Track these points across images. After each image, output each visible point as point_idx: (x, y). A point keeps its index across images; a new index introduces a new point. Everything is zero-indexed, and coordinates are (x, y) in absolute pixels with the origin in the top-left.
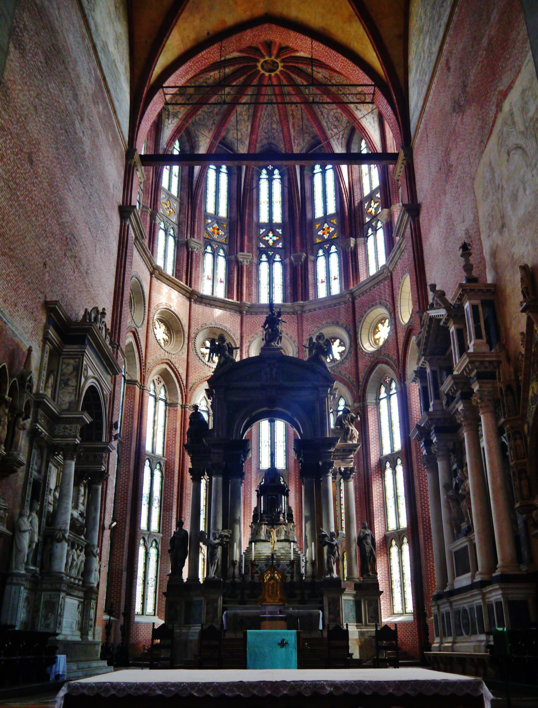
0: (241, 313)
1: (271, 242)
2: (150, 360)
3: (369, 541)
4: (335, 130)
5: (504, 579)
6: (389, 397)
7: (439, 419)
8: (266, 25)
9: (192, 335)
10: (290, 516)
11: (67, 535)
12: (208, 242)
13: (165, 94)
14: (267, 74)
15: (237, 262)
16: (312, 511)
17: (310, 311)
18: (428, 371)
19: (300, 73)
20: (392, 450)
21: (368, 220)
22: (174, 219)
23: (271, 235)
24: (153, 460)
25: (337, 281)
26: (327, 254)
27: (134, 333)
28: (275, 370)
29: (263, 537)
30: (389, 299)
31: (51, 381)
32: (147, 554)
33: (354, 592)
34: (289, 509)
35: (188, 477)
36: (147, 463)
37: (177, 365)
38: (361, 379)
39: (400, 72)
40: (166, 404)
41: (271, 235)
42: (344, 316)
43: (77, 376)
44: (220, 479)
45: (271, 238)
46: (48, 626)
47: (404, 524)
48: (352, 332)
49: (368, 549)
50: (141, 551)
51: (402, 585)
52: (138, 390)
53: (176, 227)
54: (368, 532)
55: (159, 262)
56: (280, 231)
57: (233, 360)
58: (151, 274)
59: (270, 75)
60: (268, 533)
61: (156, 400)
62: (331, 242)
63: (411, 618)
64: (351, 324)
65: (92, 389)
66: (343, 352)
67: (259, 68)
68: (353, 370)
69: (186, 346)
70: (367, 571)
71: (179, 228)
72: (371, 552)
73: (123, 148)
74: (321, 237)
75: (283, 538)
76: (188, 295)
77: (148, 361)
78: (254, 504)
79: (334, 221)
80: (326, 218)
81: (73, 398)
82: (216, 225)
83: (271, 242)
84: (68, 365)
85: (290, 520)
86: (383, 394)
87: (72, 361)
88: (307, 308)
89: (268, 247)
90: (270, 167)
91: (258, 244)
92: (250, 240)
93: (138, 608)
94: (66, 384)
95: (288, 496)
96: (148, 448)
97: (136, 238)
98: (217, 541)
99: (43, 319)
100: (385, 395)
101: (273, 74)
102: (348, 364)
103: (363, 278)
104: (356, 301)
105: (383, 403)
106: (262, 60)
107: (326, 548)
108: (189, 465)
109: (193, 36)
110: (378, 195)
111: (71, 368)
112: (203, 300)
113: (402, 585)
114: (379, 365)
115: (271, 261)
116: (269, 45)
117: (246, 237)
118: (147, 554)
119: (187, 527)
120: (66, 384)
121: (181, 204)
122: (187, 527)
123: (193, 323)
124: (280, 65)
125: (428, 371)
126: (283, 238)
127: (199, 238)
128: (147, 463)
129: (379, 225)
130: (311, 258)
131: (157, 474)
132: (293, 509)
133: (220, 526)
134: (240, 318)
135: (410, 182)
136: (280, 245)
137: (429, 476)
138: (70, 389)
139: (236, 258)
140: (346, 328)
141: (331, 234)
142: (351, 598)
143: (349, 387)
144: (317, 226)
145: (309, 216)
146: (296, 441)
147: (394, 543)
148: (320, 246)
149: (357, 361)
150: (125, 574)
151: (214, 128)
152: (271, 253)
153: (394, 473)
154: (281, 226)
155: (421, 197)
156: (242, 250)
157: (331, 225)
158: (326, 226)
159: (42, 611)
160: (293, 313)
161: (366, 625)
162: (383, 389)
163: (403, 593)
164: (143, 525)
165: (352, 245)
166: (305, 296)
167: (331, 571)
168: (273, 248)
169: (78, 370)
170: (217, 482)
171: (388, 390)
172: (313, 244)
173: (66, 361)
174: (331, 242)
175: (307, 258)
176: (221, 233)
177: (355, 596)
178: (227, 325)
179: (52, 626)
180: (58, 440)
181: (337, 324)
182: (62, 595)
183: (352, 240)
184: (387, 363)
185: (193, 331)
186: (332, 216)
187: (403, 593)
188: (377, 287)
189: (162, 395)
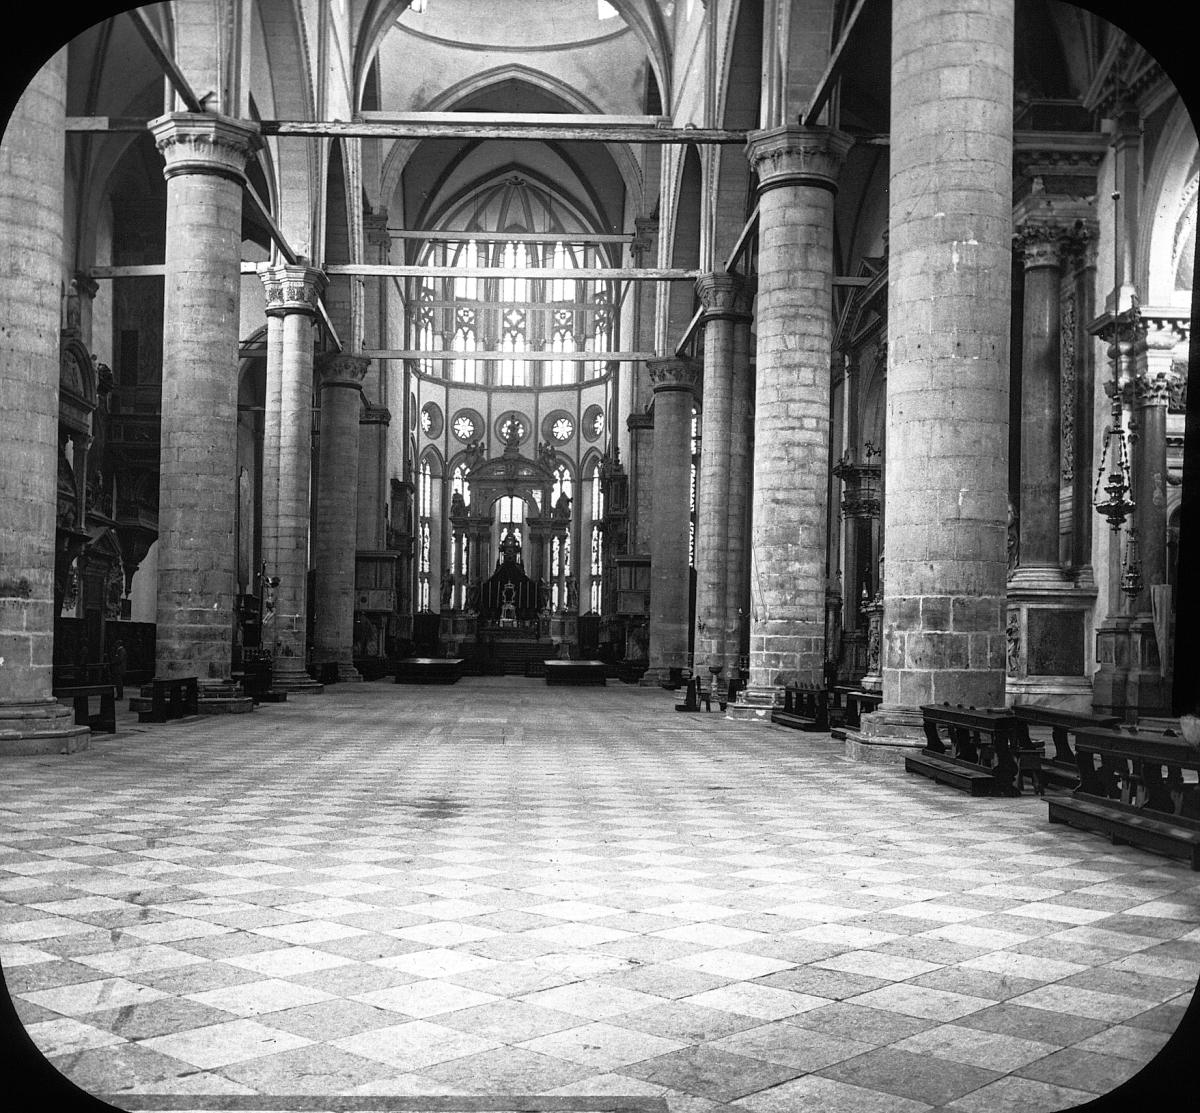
112: (457, 385)
152: (514, 333)
185: (451, 415)
189: (428, 472)
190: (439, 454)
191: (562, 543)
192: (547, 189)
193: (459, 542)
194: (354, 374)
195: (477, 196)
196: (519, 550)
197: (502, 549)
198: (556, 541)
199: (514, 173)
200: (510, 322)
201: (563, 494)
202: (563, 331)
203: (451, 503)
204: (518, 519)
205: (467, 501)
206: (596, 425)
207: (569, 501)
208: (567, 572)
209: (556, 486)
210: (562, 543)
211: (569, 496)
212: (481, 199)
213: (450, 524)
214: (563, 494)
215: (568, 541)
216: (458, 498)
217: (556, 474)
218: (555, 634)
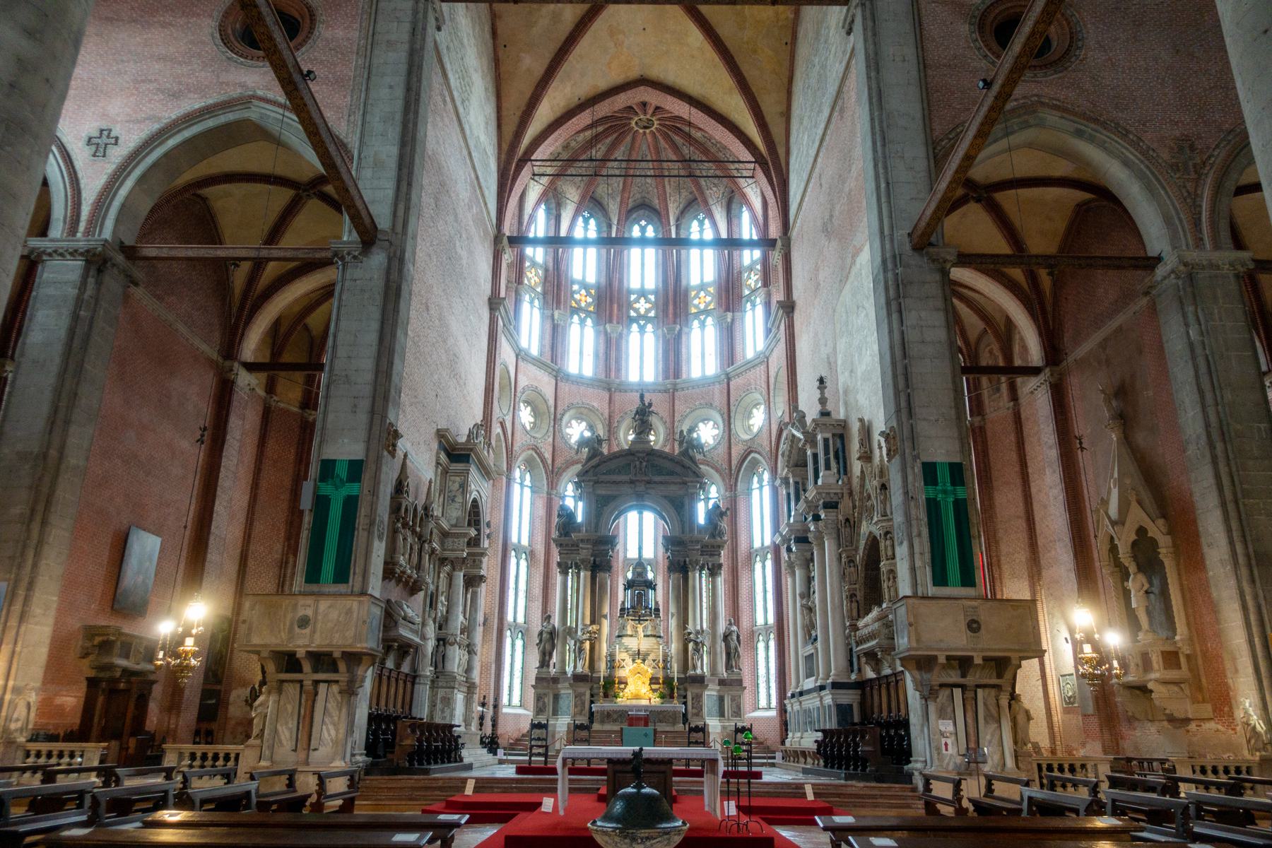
0: (609, 390)
1: (642, 311)
2: (516, 448)
3: (735, 638)
4: (715, 189)
5: (836, 686)
6: (761, 487)
7: (798, 530)
8: (642, 88)
9: (559, 416)
10: (657, 610)
11: (458, 639)
12: (576, 311)
13: (533, 166)
14: (641, 131)
15: (606, 333)
16: (678, 608)
17: (683, 389)
18: (791, 481)
19: (678, 130)
20: (763, 544)
21: (747, 292)
22: (539, 289)
23: (642, 300)
24: (518, 549)
25: (713, 357)
26: (703, 325)
27: (501, 423)
28: (644, 464)
29: (629, 632)
30: (764, 386)
31: (441, 499)
32: (513, 645)
33: (718, 688)
34: (657, 603)
35: (556, 571)
36: (513, 553)
37: (543, 450)
38: (733, 468)
39: (781, 151)
40: (533, 492)
41: (642, 300)
42: (719, 399)
43: (463, 493)
44: (589, 573)
45: (642, 306)
46: (444, 718)
47: (771, 620)
48: (726, 416)
49: (733, 645)
50: (508, 641)
51: (768, 681)
52: (504, 478)
53: (541, 297)
54: (734, 628)
55: (524, 343)
56: (652, 298)
57: (602, 453)
58: (517, 356)
59: (645, 133)
60: (635, 628)
61: (522, 485)
62: (706, 312)
63: (773, 713)
64: (726, 407)
65: (475, 501)
66: (717, 435)
67: (633, 123)
68: (726, 457)
69: (551, 429)
70: (732, 667)
71: (544, 298)
72: (736, 649)
73: (492, 232)
74: (697, 307)
75: (649, 633)
76: (554, 373)
77: (515, 448)
78: (621, 598)
79: (711, 290)
80: (702, 287)
81: (460, 513)
82: (583, 292)
83: (642, 311)
84: (454, 482)
85: (657, 616)
86: (755, 485)
87: (458, 479)
88: (679, 386)
89: (640, 317)
90: (643, 223)
91: (628, 312)
92: (620, 308)
93: (505, 700)
94: (453, 501)
95: (655, 590)
96: (514, 539)
97: (504, 325)
98: (585, 637)
99: (435, 445)
100: (758, 486)
101: (648, 131)
102: (722, 450)
103: (739, 362)
104: (732, 383)
105: (755, 494)
106: (636, 119)
107: (691, 646)
108: (556, 557)
109: (562, 104)
110: (759, 267)
111: (457, 485)
112: (568, 378)
113: (768, 681)
114: (753, 455)
115: (642, 329)
116: (644, 105)
117: (615, 306)
118: (513, 645)
119: (556, 621)
120: (453, 501)
121: (546, 270)
122: (556, 621)
123: (559, 403)
124: (656, 123)
125: (791, 481)
126: (655, 305)
127: (565, 308)
128: (513, 553)
129: (758, 300)
130: (685, 330)
131: (523, 564)
132: (661, 603)
133: (588, 622)
134: (608, 395)
135: (787, 275)
136: (652, 314)
137: (789, 580)
138: (457, 505)
139: (605, 329)
140: (720, 411)
141: (707, 304)
142: (715, 693)
143: (721, 475)
144: (693, 294)
145: (684, 283)
146: (665, 537)
147: (761, 638)
148: (697, 315)
149: (730, 448)
150: (493, 666)
151: (582, 185)
152: (642, 323)
153: (764, 567)
154: (656, 292)
155: (796, 295)
156: (611, 321)
157: (708, 293)
158: (702, 294)
159: (439, 706)
160: (665, 391)
161: (729, 719)
162: (755, 479)
163: (769, 688)
164: (510, 618)
165: (729, 320)
166: (677, 374)
167: (695, 668)
168: (645, 317)
169: (464, 487)
170: (585, 577)
171: (760, 481)
173: (452, 478)
174: (706, 312)
175: (680, 330)
176: (589, 300)
177: (719, 691)
178: (595, 404)
179: (448, 718)
180: (447, 554)
181: (711, 406)
182: (456, 691)
183: (729, 315)
184: (759, 453)
186: (709, 285)
187: (769, 688)
188: (753, 371)
189: (528, 482)
190: (543, 460)
196: (651, 585)
197: (629, 585)
200: (636, 310)
202: (702, 317)
203: (555, 520)
204: (648, 553)
205: (579, 519)
206: (751, 422)
207: (722, 514)
218: (710, 715)
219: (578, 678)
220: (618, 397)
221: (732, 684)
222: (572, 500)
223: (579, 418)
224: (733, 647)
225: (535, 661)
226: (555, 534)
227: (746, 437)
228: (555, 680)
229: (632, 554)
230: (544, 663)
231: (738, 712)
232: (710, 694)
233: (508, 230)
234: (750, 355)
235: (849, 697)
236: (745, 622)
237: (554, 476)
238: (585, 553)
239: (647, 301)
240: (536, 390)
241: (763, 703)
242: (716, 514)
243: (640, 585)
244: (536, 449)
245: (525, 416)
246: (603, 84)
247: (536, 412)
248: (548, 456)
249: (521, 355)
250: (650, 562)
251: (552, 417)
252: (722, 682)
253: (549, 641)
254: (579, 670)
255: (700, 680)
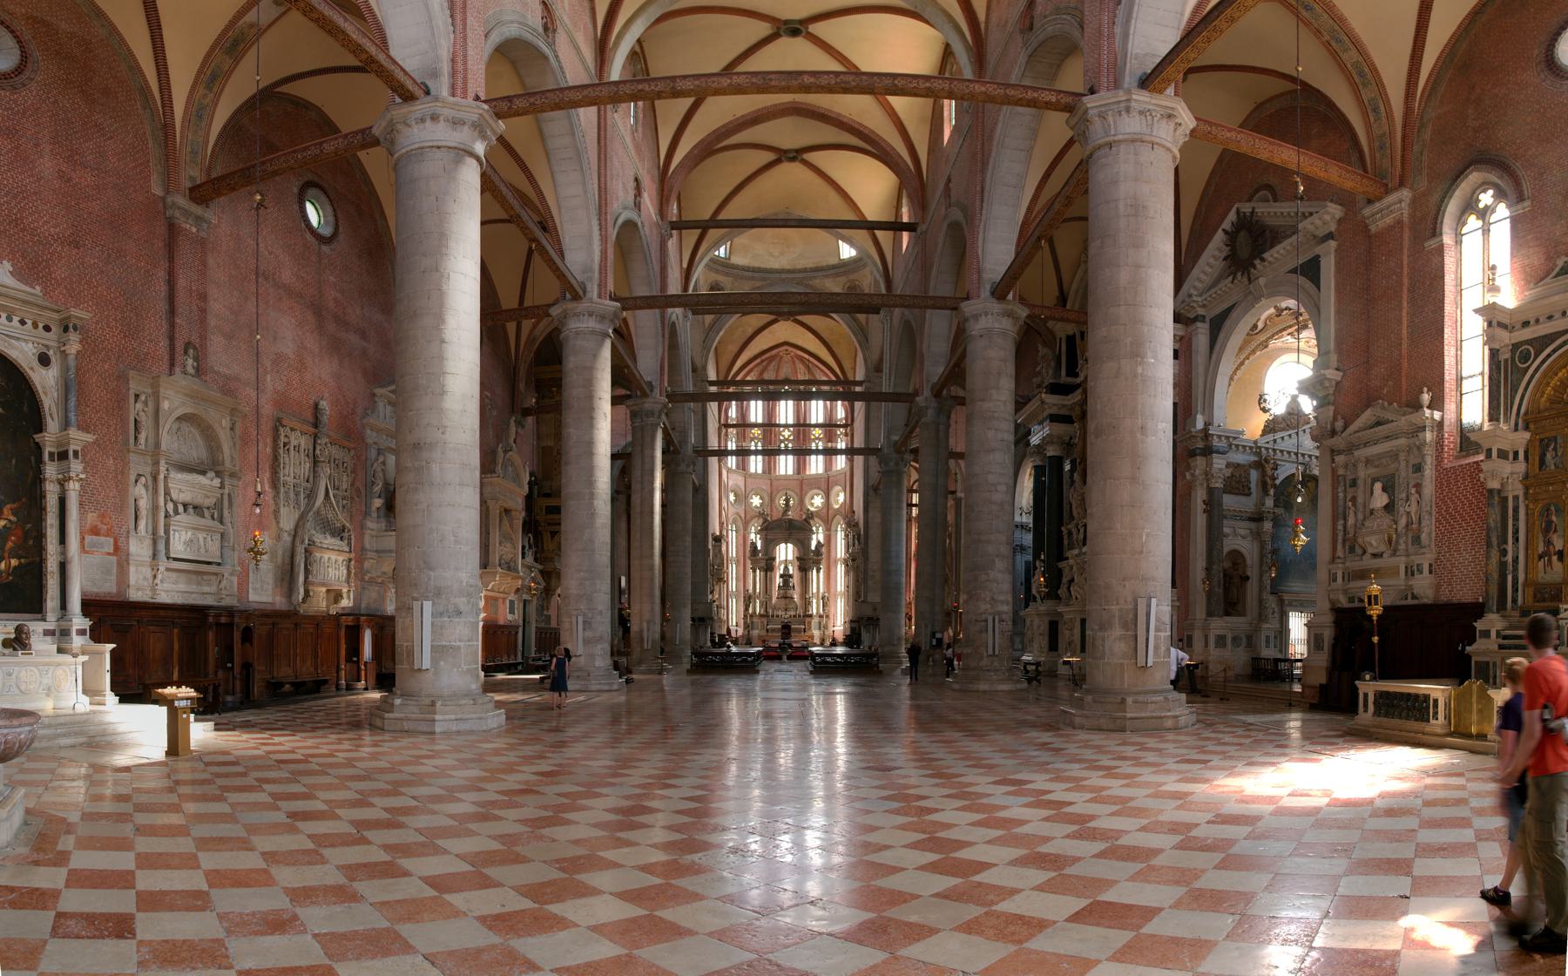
12: (752, 439)
42: (824, 486)
89: (787, 440)
92: (775, 436)
102: (825, 511)
103: (834, 469)
112: (751, 475)
119: (751, 591)
122: (751, 591)
136: (791, 438)
148: (814, 440)
172: (810, 439)
181: (819, 488)
190: (740, 517)
191: (818, 571)
192: (807, 356)
193: (754, 571)
194: (688, 466)
195: (763, 361)
196: (791, 576)
197: (781, 576)
198: (815, 571)
199: (785, 347)
201: (819, 542)
203: (748, 549)
204: (790, 557)
205: (759, 548)
208: (821, 591)
209: (814, 537)
210: (818, 571)
211: (822, 541)
212: (764, 364)
213: (749, 562)
214: (819, 542)
215: (822, 571)
216: (754, 545)
217: (814, 529)
219: (761, 616)
220: (775, 483)
221: (825, 616)
222: (755, 537)
223: (756, 494)
224: (826, 602)
225: (742, 609)
226: (748, 554)
227: (837, 507)
228: (751, 616)
229: (783, 558)
230: (746, 609)
231: (826, 627)
232: (815, 621)
233: (722, 422)
234: (839, 468)
235: (854, 625)
236: (832, 590)
237: (746, 524)
238: (763, 564)
239: (789, 431)
240: (736, 485)
241: (839, 624)
242: (819, 544)
243: (786, 577)
244: (737, 514)
245: (732, 498)
246: (765, 347)
247: (736, 495)
248: (743, 516)
249: (729, 470)
250: (791, 562)
251: (742, 498)
252: (821, 616)
253: (748, 600)
254: (762, 612)
255: (811, 616)
